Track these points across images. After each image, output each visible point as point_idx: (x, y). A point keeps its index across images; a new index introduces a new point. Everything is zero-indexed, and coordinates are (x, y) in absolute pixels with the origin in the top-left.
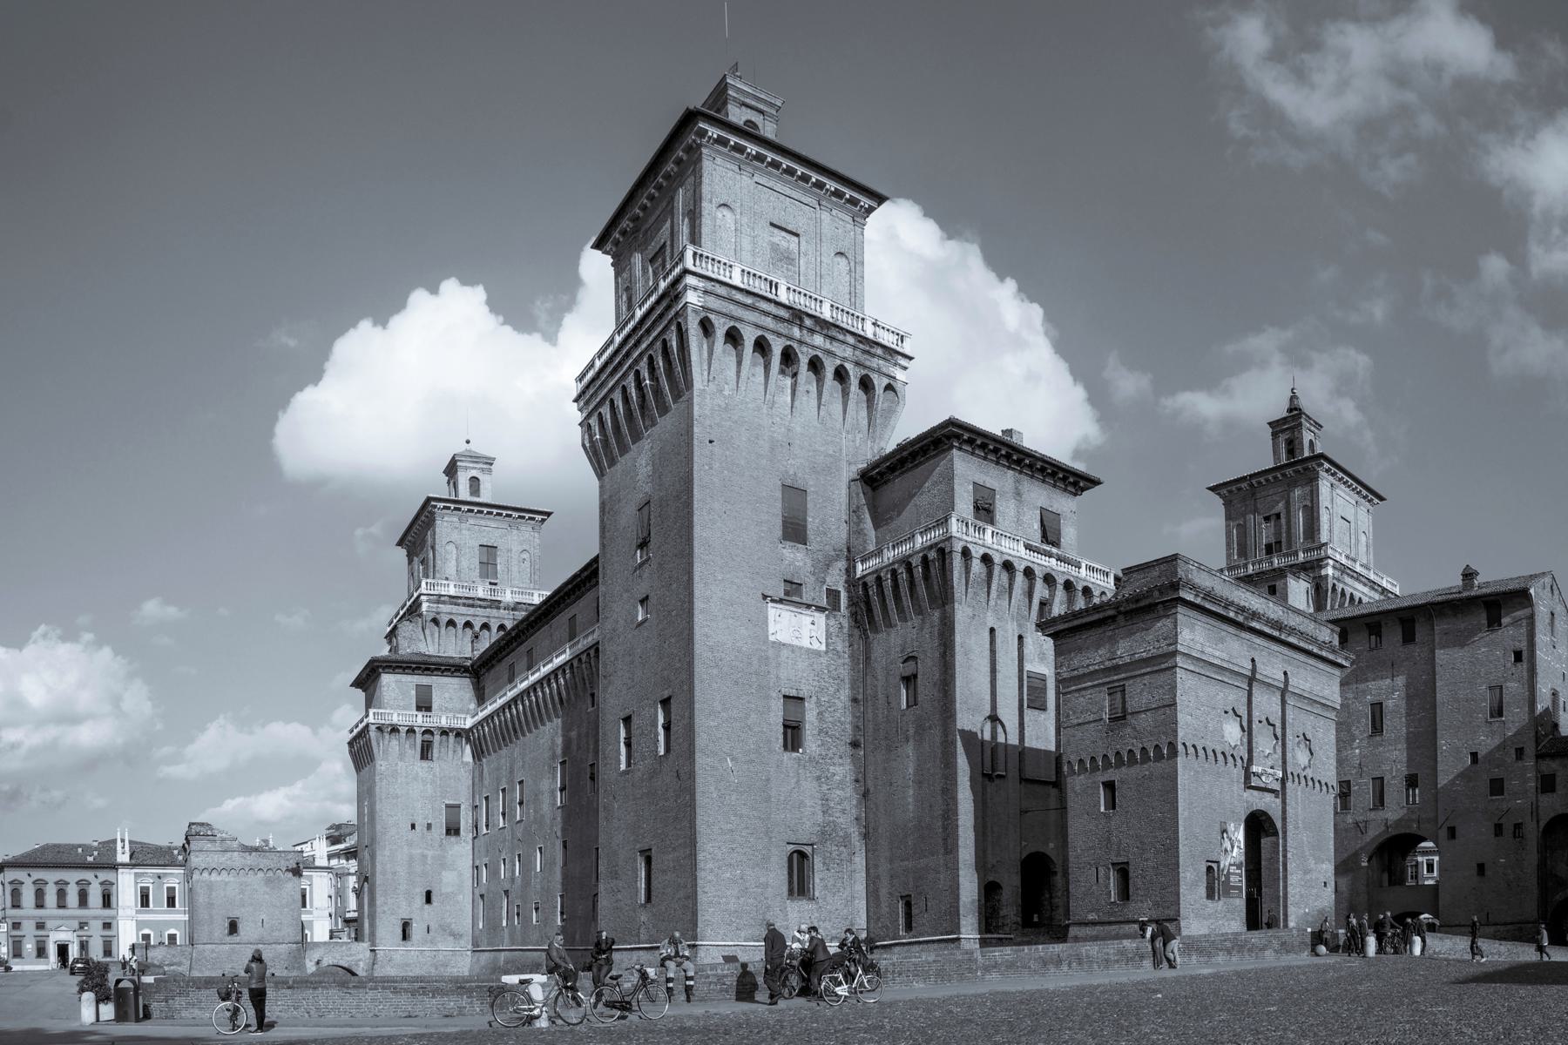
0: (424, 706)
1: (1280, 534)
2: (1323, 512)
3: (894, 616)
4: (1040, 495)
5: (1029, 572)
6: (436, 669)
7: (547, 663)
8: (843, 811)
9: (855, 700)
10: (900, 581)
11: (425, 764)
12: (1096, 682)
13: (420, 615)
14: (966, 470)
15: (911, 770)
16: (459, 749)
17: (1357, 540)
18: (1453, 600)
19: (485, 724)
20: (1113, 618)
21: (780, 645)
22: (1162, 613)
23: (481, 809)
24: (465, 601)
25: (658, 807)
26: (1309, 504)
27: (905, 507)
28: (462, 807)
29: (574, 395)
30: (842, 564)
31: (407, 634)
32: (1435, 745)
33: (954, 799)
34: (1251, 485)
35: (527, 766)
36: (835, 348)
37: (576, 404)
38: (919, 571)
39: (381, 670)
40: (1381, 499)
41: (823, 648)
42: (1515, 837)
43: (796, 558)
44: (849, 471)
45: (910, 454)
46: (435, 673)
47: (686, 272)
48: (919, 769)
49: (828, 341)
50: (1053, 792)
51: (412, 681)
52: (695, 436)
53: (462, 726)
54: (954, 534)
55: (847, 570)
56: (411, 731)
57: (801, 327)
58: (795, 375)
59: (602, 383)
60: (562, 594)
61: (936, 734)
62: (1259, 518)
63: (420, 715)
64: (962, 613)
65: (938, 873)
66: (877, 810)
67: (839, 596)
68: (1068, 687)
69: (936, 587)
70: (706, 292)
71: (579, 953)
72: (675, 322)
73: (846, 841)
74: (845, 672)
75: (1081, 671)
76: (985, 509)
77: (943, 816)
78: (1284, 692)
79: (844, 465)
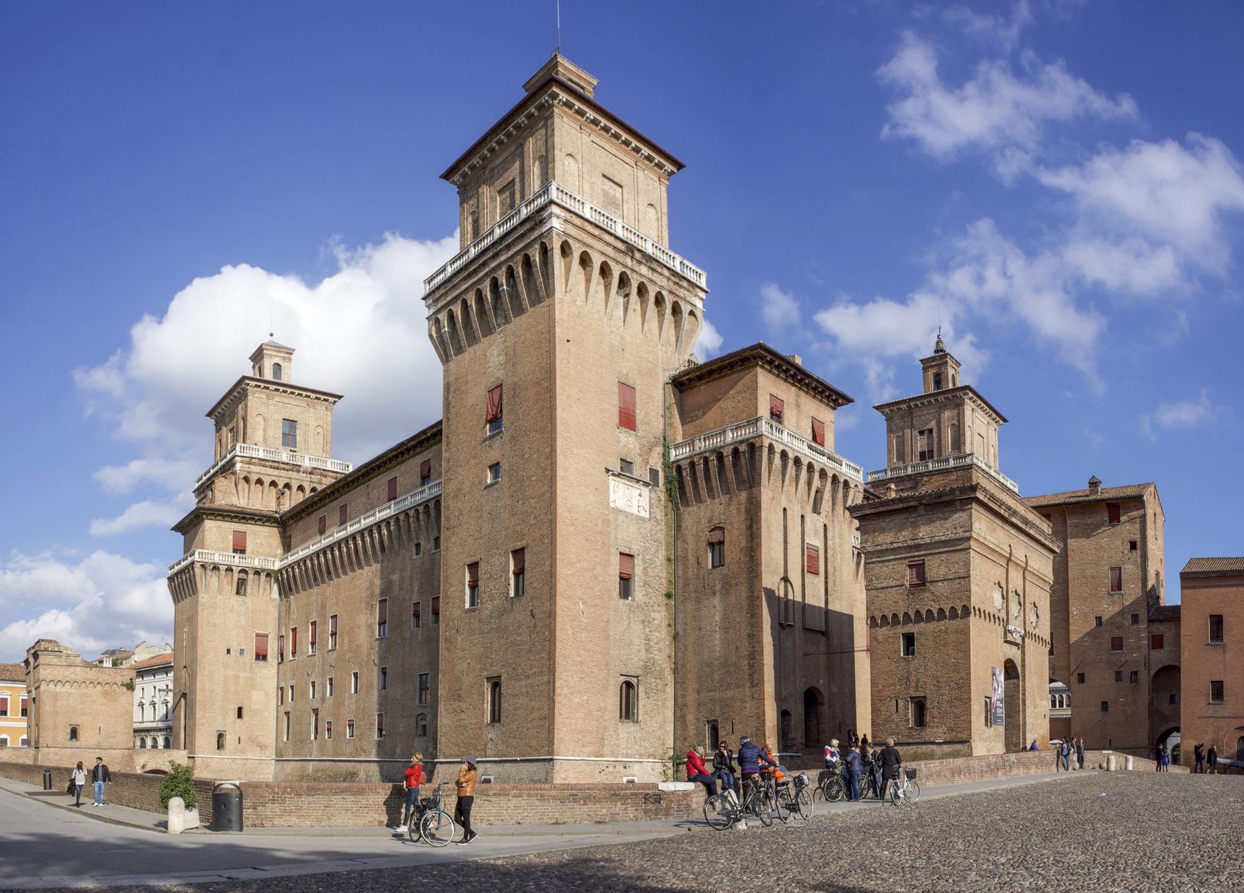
0: (240, 549)
1: (932, 444)
2: (967, 428)
3: (704, 493)
4: (813, 408)
5: (810, 467)
6: (219, 515)
7: (369, 517)
8: (660, 650)
9: (669, 560)
10: (711, 466)
11: (240, 598)
12: (898, 556)
13: (234, 473)
14: (767, 385)
15: (717, 618)
16: (268, 587)
17: (988, 451)
18: (1083, 502)
19: (296, 567)
20: (914, 508)
21: (619, 511)
22: (959, 507)
23: (288, 638)
24: (271, 464)
25: (509, 641)
26: (956, 423)
27: (710, 409)
28: (270, 636)
29: (423, 294)
30: (659, 449)
31: (222, 489)
32: (1067, 609)
33: (760, 642)
34: (909, 407)
35: (340, 603)
36: (655, 277)
37: (424, 301)
38: (729, 461)
39: (205, 517)
40: (1005, 420)
41: (647, 516)
42: (1131, 682)
43: (629, 443)
44: (664, 377)
45: (718, 367)
46: (250, 522)
47: (552, 202)
48: (725, 618)
49: (651, 272)
50: (823, 639)
51: (230, 527)
52: (557, 335)
53: (272, 568)
54: (764, 433)
55: (664, 455)
56: (229, 569)
57: (632, 258)
58: (627, 295)
59: (454, 286)
60: (385, 459)
61: (743, 591)
62: (916, 433)
63: (237, 556)
64: (767, 493)
65: (745, 702)
66: (686, 649)
67: (658, 475)
68: (871, 558)
69: (745, 474)
70: (566, 221)
71: (400, 764)
72: (539, 242)
73: (660, 676)
74: (661, 536)
75: (884, 547)
76: (777, 415)
77: (750, 656)
78: (1025, 569)
79: (660, 370)
